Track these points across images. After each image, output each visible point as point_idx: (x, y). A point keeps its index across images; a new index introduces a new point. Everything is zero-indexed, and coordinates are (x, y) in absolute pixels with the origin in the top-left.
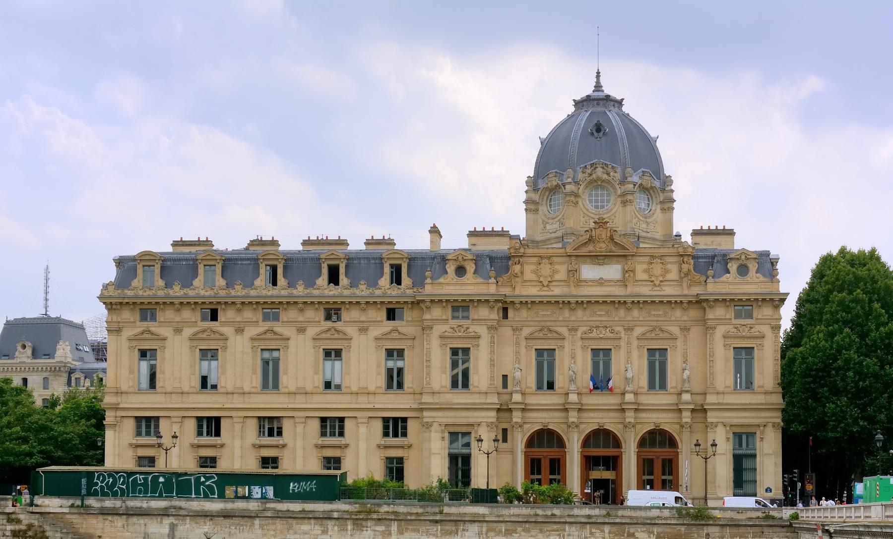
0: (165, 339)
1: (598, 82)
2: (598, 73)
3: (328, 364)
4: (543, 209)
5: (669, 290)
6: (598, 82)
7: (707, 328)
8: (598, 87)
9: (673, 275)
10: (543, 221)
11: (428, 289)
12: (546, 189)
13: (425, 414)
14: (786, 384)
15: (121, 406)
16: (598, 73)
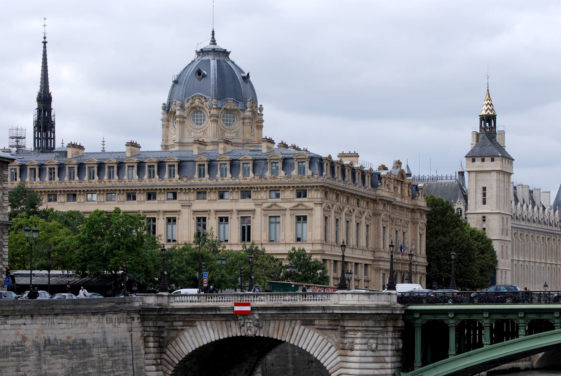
0: (312, 209)
1: (213, 38)
2: (213, 32)
3: (299, 225)
4: (220, 121)
5: (406, 202)
6: (213, 38)
7: (415, 223)
8: (213, 42)
9: (407, 195)
10: (221, 129)
11: (379, 192)
12: (225, 109)
13: (381, 263)
14: (427, 253)
15: (326, 252)
16: (213, 32)
